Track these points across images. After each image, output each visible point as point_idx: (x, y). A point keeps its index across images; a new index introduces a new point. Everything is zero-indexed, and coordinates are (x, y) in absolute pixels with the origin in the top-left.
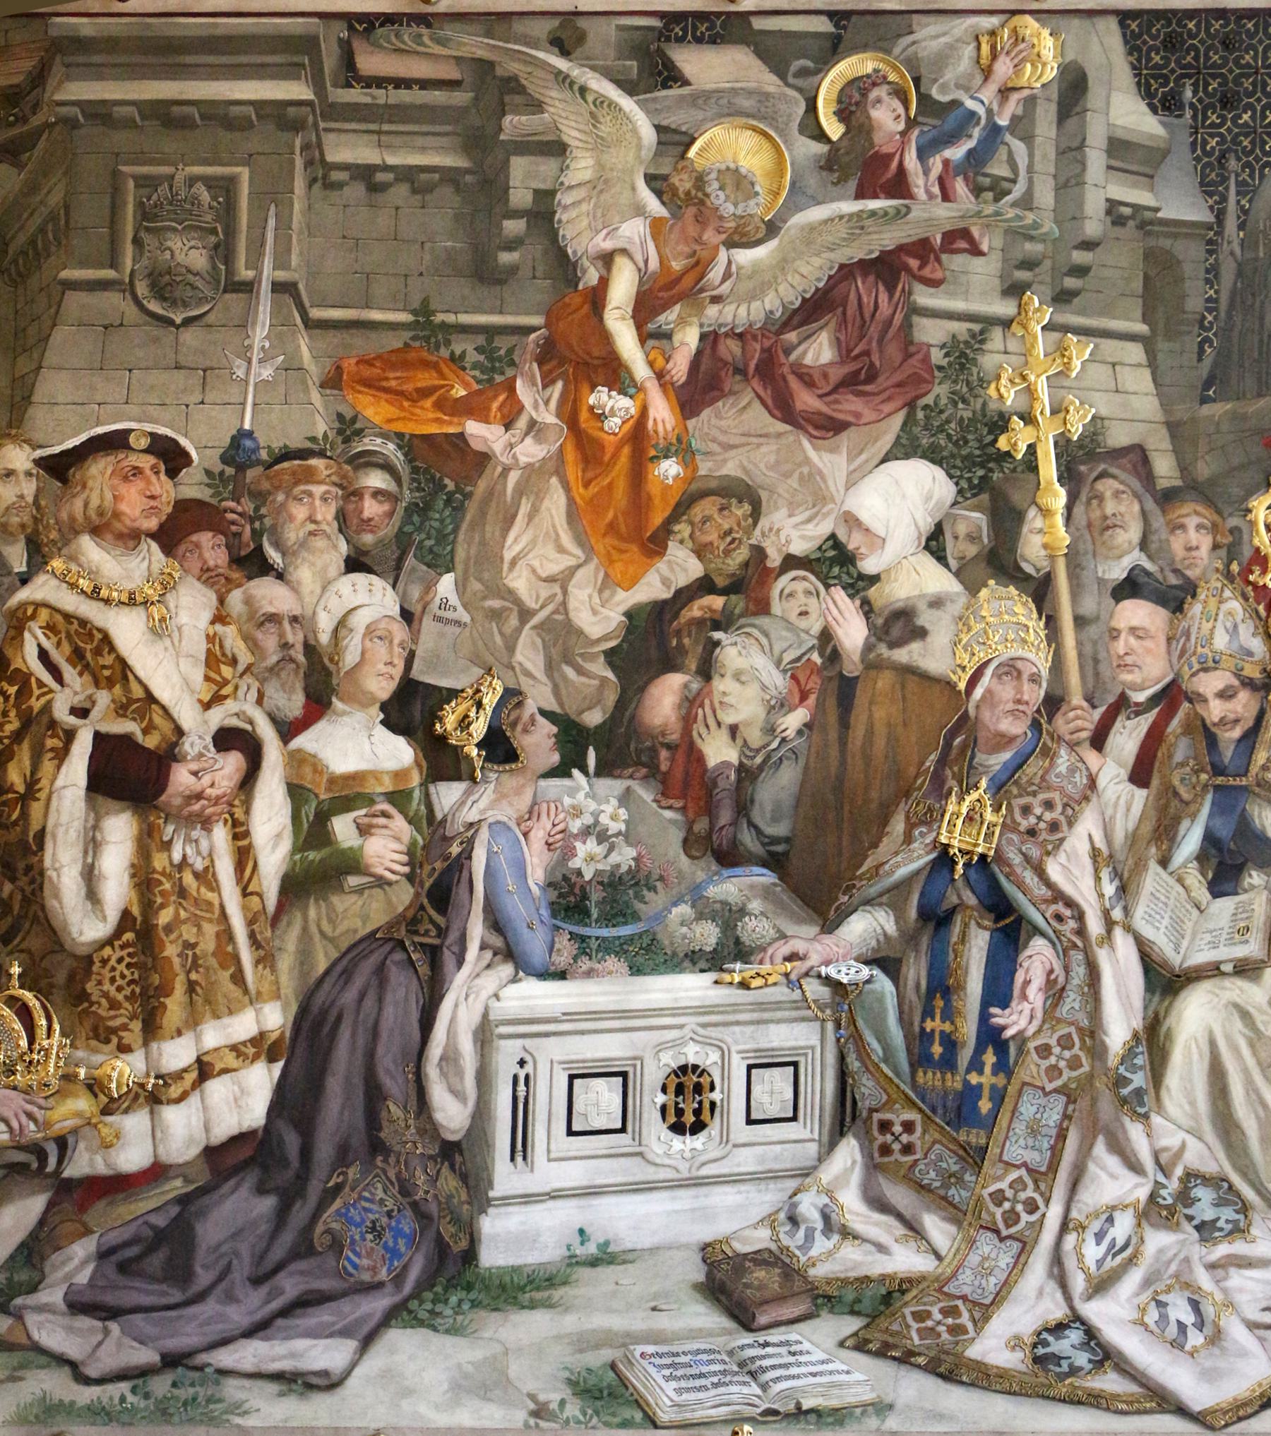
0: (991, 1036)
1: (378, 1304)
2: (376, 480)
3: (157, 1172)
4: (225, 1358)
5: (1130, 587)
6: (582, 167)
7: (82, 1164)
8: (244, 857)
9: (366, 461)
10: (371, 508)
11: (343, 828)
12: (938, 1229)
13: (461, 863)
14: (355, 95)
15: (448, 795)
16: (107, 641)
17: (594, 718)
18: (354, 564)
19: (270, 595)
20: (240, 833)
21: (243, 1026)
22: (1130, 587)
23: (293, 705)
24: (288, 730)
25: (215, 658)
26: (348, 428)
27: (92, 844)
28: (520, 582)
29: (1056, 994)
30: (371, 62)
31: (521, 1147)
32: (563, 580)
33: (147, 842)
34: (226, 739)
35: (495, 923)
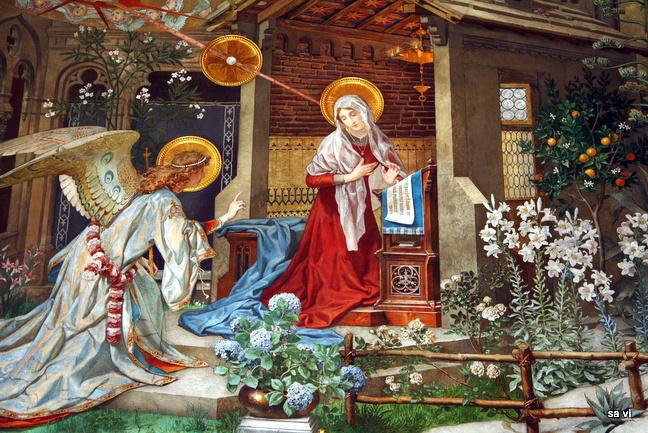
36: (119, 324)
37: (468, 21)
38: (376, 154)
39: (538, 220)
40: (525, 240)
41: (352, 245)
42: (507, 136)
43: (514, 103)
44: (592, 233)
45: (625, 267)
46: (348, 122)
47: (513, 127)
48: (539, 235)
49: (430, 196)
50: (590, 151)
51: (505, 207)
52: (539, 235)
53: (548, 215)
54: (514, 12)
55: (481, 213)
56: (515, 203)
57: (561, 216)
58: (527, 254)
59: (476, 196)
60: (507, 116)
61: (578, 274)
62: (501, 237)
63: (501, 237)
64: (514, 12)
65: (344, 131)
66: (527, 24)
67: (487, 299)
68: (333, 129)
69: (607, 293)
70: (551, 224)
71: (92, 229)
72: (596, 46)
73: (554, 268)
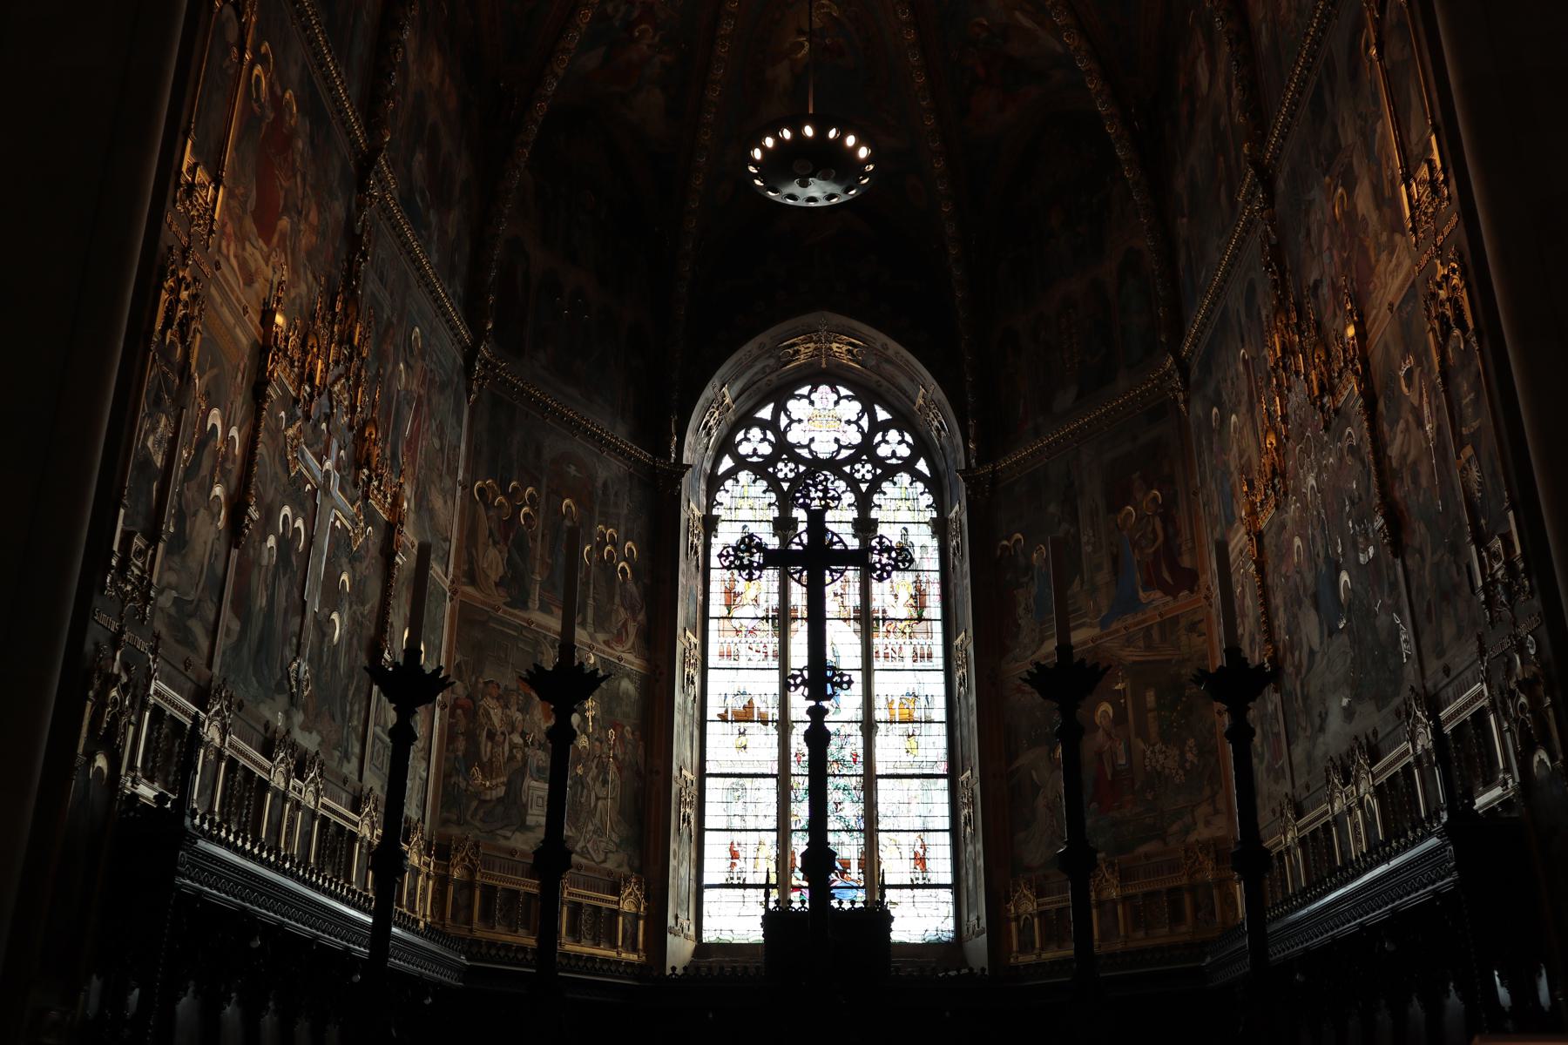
0: (580, 802)
1: (514, 827)
2: (521, 698)
3: (491, 801)
4: (498, 832)
5: (597, 739)
6: (545, 658)
7: (482, 798)
8: (503, 753)
9: (520, 694)
10: (520, 702)
11: (515, 751)
12: (573, 830)
13: (527, 760)
14: (521, 637)
15: (526, 749)
16: (489, 714)
17: (543, 742)
18: (518, 710)
19: (508, 712)
20: (503, 749)
21: (502, 780)
22: (597, 739)
23: (510, 730)
24: (509, 734)
25: (502, 720)
26: (518, 689)
27: (486, 746)
28: (536, 718)
29: (587, 797)
30: (524, 633)
31: (531, 807)
32: (540, 719)
33: (492, 748)
34: (503, 733)
35: (530, 770)
36: (1053, 826)
37: (1135, 662)
38: (1113, 736)
39: (1161, 752)
40: (1157, 761)
41: (1109, 777)
42: (1150, 715)
43: (1150, 697)
44: (1178, 752)
45: (1188, 765)
46: (1104, 723)
47: (1150, 711)
48: (1161, 757)
49: (1129, 749)
50: (1175, 714)
51: (1151, 748)
52: (1161, 757)
53: (1164, 749)
54: (1147, 654)
55: (1144, 751)
56: (1154, 745)
57: (1167, 747)
58: (1158, 768)
59: (1142, 746)
60: (1149, 705)
61: (1174, 771)
62: (1151, 761)
63: (1151, 761)
64: (1147, 654)
65: (1104, 729)
66: (1151, 658)
67: (1149, 790)
68: (1099, 728)
69: (1183, 778)
70: (1165, 752)
71: (1042, 790)
72: (1174, 661)
73: (1167, 771)
